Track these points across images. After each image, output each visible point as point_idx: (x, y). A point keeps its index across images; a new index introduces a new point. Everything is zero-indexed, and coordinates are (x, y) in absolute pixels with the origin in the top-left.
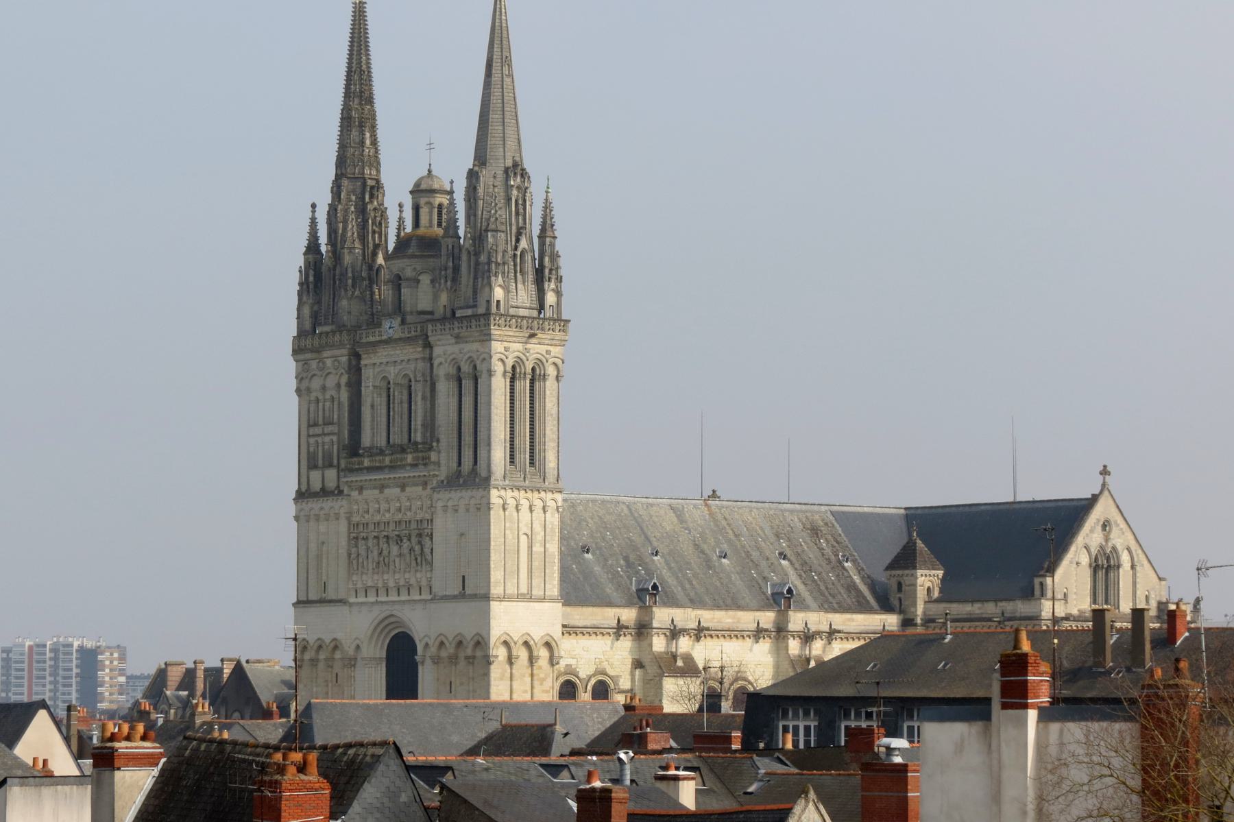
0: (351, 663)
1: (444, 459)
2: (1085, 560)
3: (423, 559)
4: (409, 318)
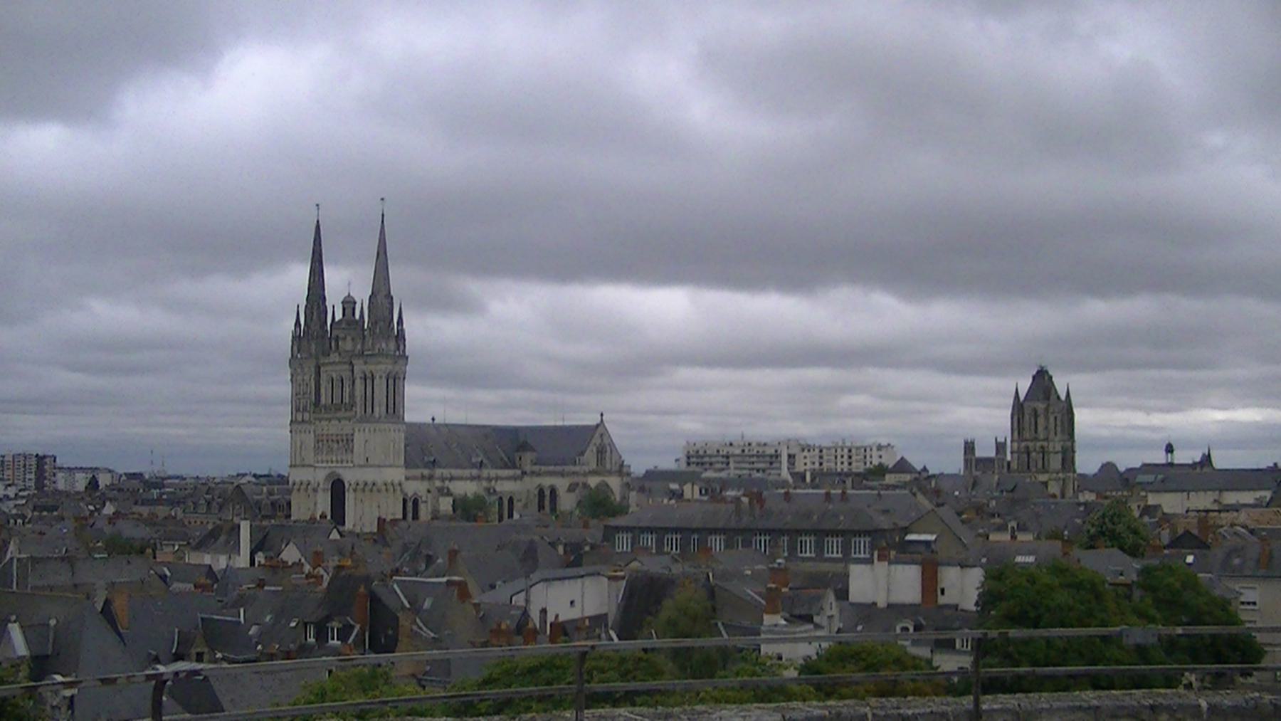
0: (315, 490)
1: (359, 409)
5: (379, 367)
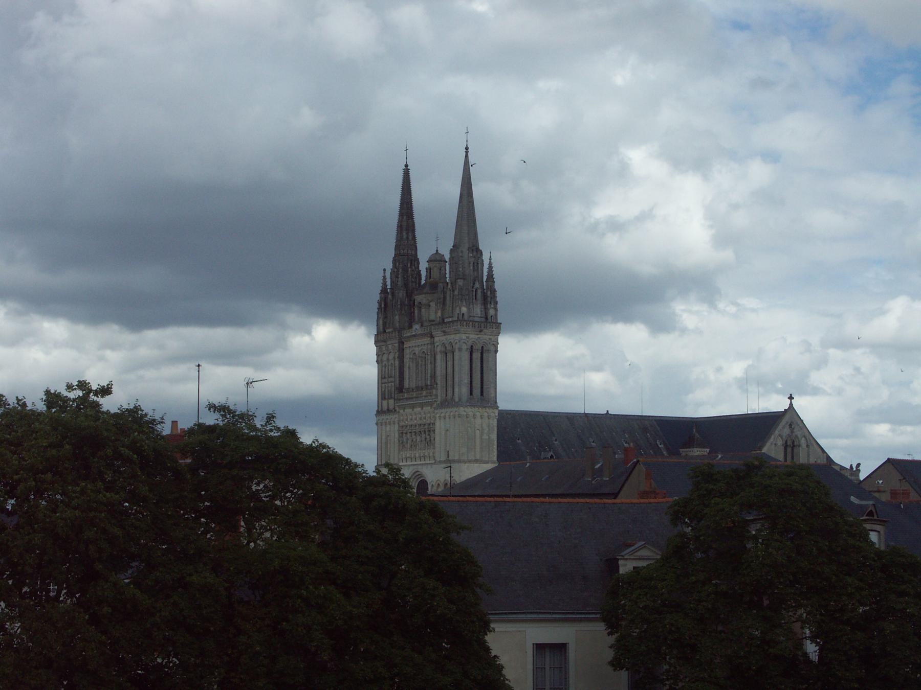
1: (439, 392)
2: (780, 442)
3: (430, 443)
4: (425, 324)
5: (457, 337)
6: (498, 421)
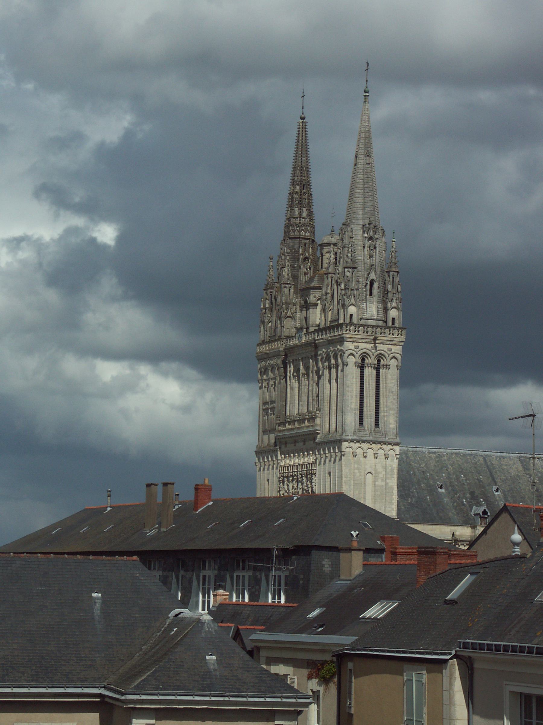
6: (400, 461)
